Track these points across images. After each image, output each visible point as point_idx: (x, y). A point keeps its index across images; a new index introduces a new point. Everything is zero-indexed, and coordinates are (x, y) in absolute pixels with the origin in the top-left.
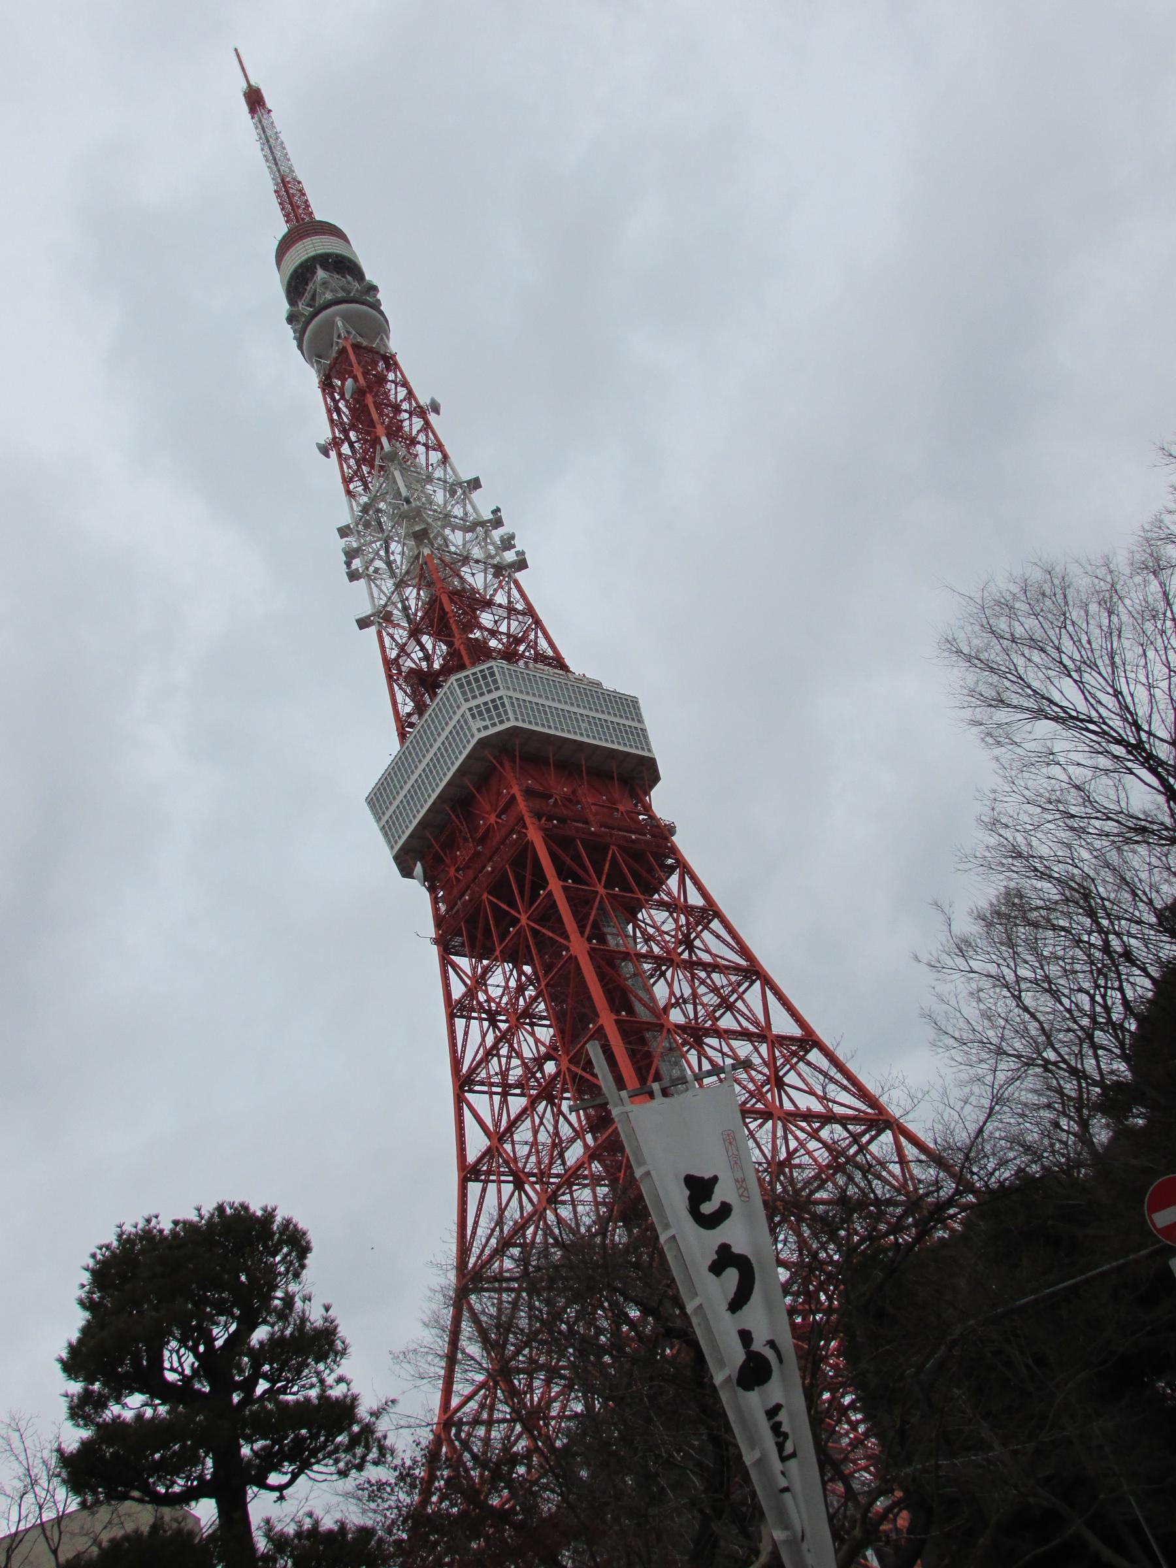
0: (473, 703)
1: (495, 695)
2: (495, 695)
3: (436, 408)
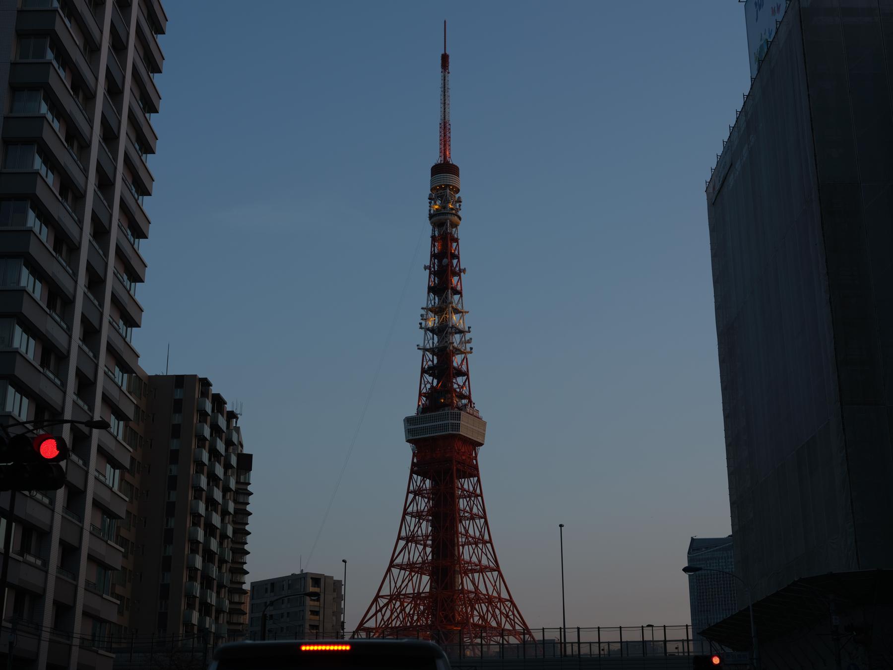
0: (452, 421)
1: (458, 422)
2: (458, 422)
3: (464, 271)
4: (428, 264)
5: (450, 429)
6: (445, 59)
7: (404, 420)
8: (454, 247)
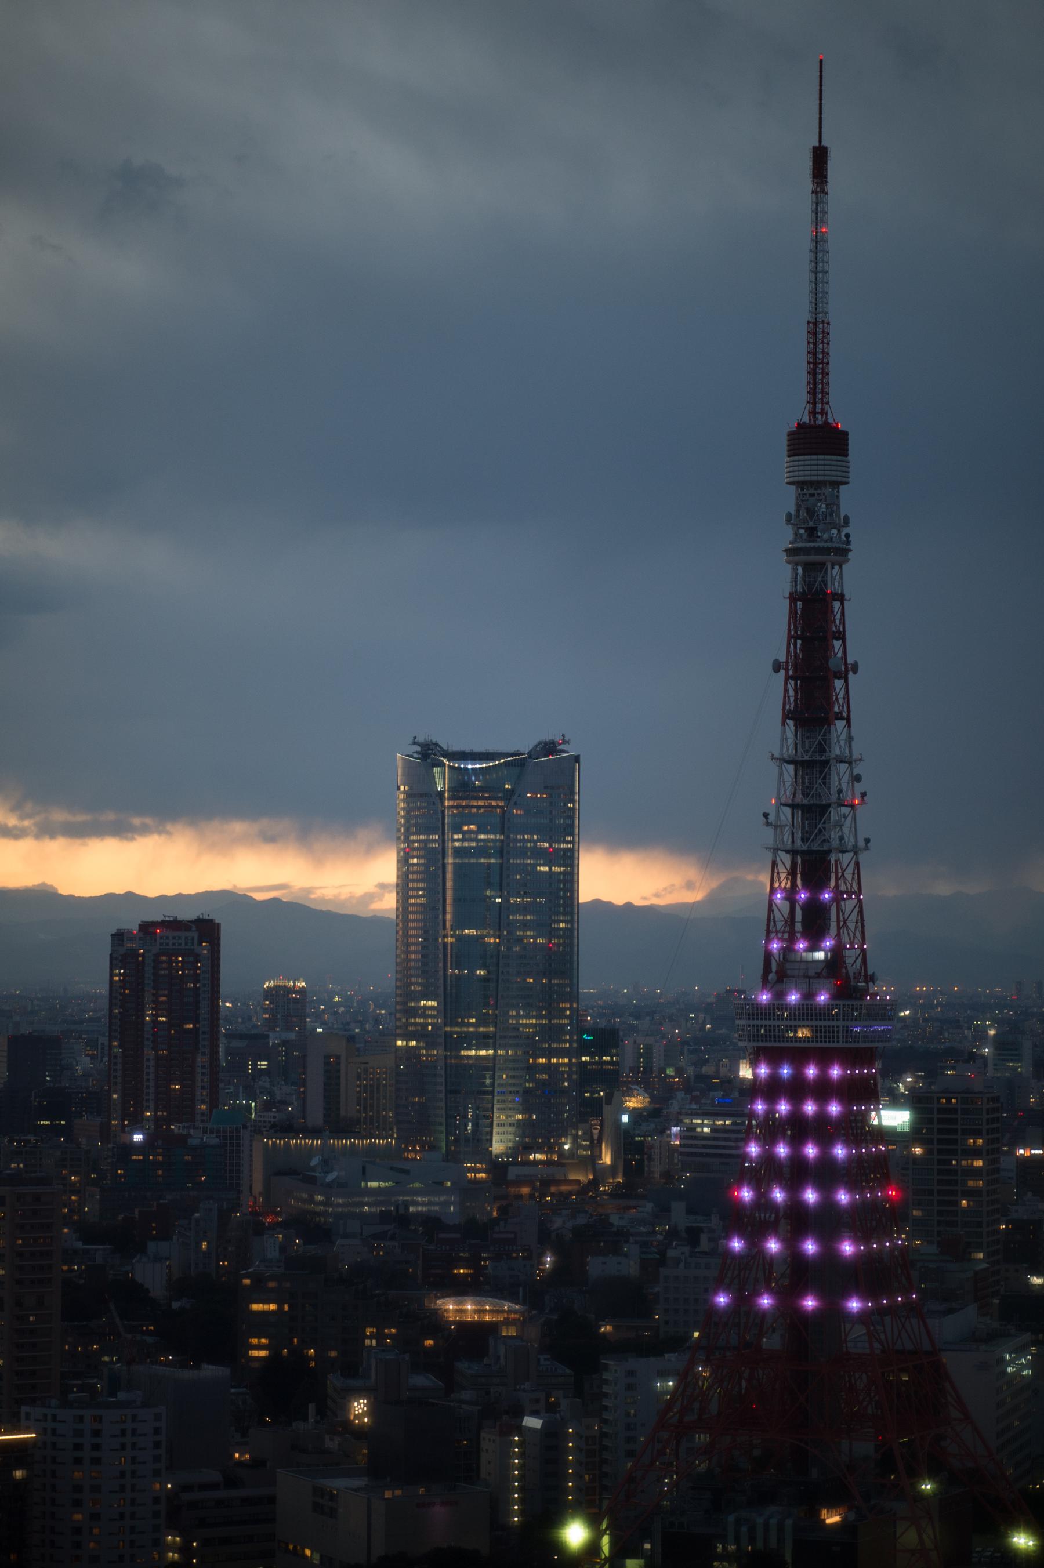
3: (855, 668)
6: (820, 156)
8: (838, 622)
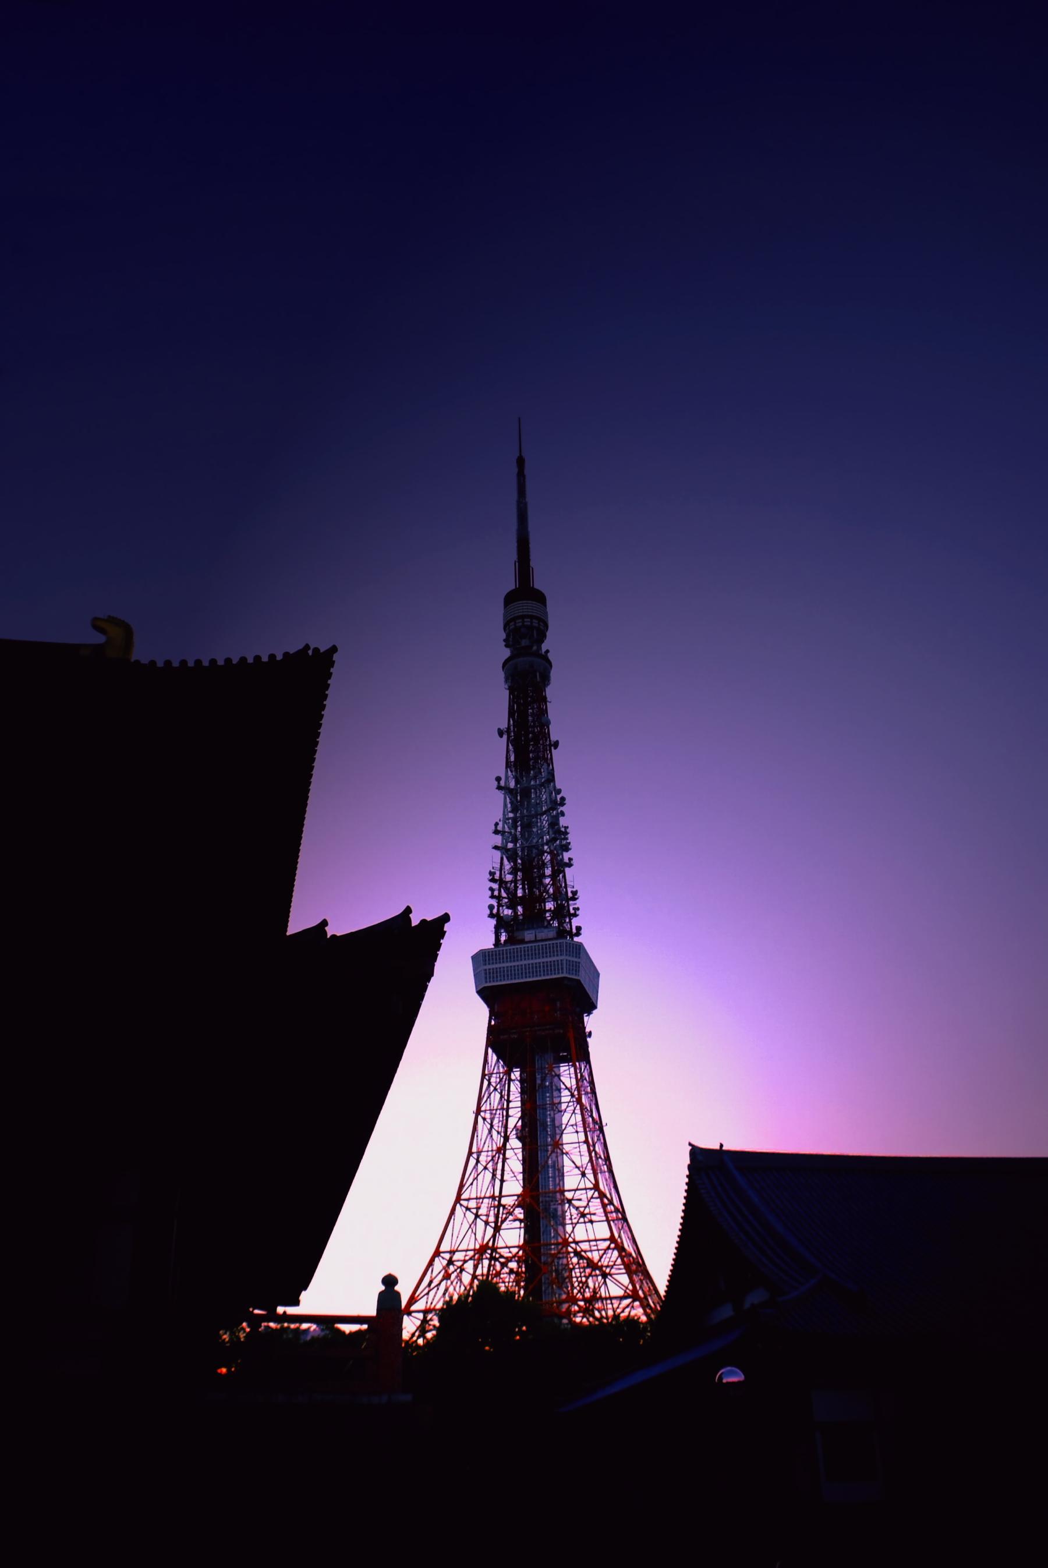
3: (556, 745)
4: (504, 726)
5: (565, 971)
6: (521, 462)
7: (474, 958)
